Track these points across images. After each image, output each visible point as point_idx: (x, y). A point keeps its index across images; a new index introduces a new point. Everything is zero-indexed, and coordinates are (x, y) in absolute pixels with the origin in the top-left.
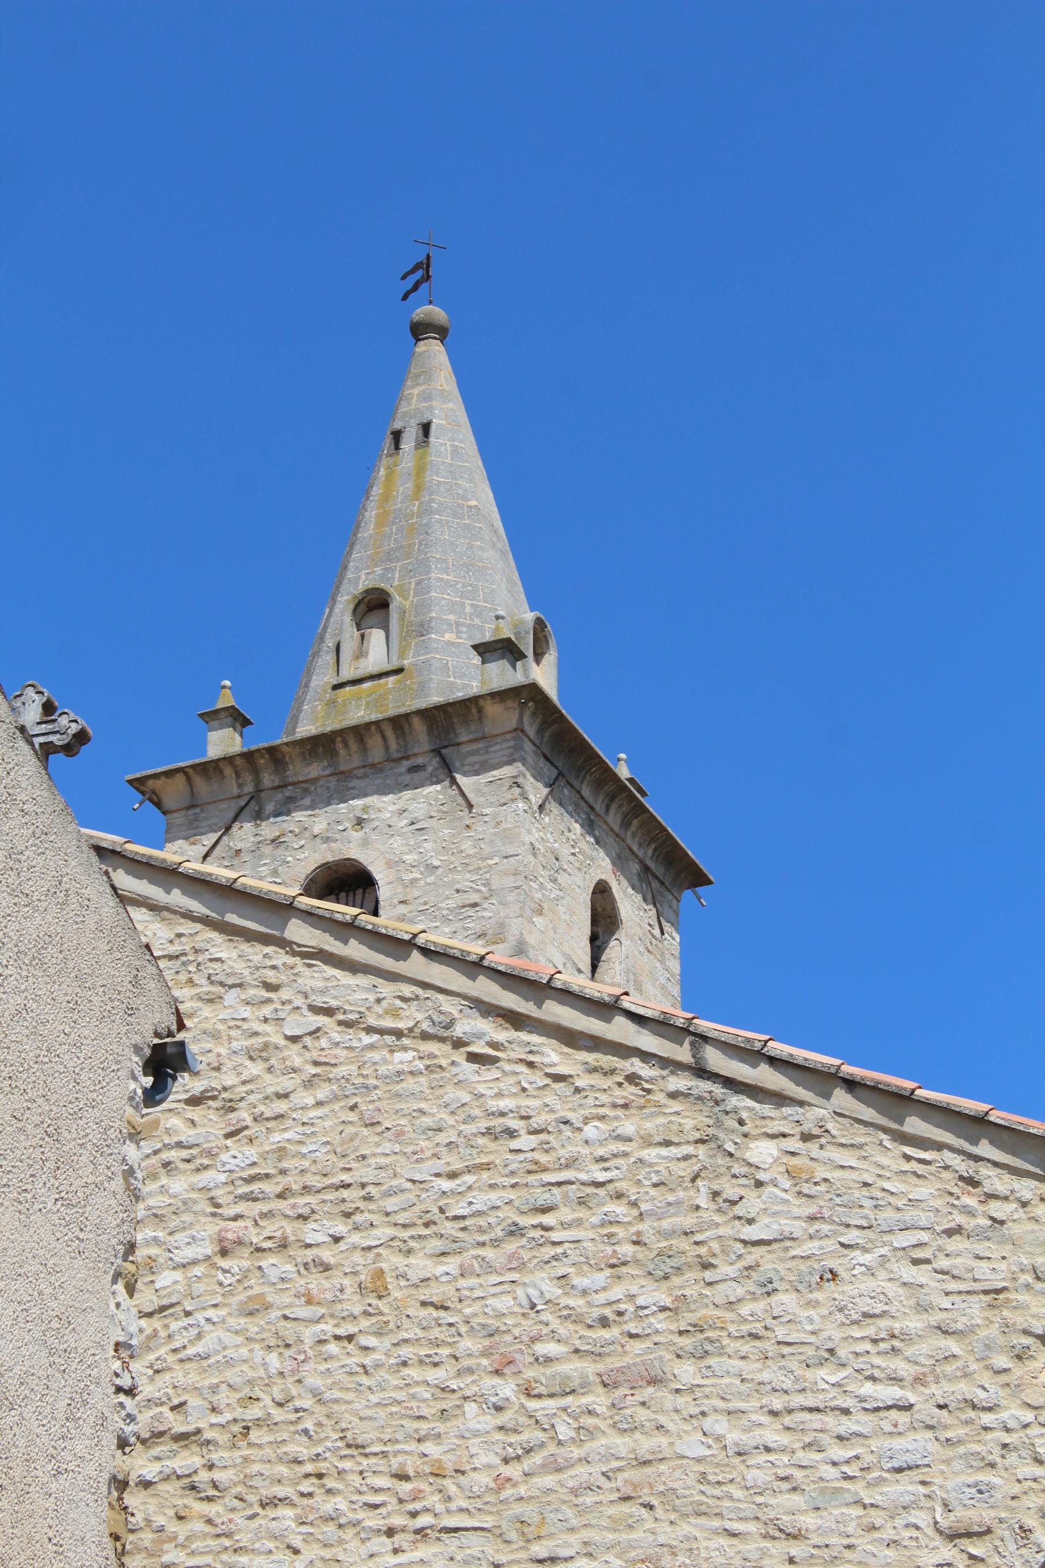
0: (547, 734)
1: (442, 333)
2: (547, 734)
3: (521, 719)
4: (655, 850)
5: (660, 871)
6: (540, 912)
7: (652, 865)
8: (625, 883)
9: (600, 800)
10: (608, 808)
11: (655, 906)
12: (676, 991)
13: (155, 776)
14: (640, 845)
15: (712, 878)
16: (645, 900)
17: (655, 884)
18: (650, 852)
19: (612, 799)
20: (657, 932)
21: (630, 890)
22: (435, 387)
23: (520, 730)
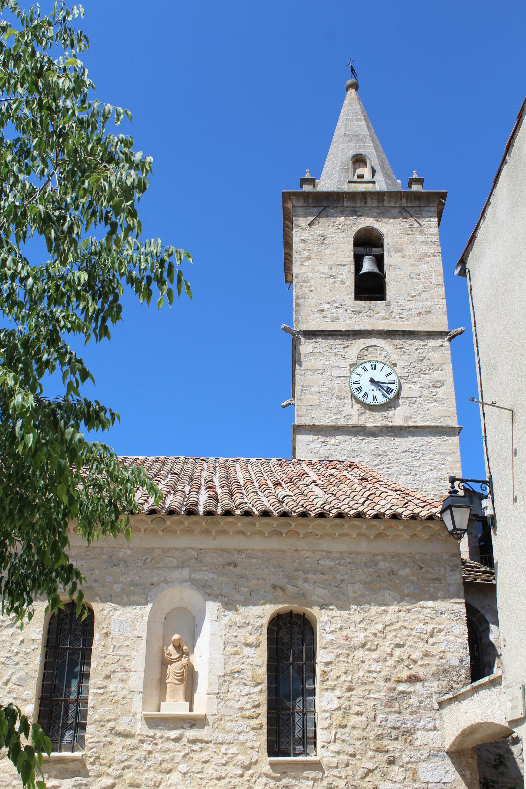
0: (310, 200)
1: (355, 86)
2: (310, 200)
3: (293, 204)
4: (407, 199)
5: (417, 203)
6: (309, 258)
7: (409, 205)
8: (386, 220)
9: (359, 202)
10: (366, 202)
11: (412, 217)
12: (436, 239)
13: (286, 278)
14: (396, 203)
15: (445, 191)
16: (405, 218)
17: (412, 211)
18: (404, 201)
19: (365, 198)
20: (416, 225)
21: (392, 220)
22: (351, 103)
23: (294, 207)
